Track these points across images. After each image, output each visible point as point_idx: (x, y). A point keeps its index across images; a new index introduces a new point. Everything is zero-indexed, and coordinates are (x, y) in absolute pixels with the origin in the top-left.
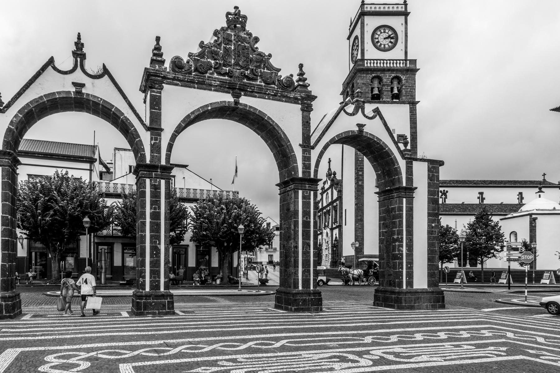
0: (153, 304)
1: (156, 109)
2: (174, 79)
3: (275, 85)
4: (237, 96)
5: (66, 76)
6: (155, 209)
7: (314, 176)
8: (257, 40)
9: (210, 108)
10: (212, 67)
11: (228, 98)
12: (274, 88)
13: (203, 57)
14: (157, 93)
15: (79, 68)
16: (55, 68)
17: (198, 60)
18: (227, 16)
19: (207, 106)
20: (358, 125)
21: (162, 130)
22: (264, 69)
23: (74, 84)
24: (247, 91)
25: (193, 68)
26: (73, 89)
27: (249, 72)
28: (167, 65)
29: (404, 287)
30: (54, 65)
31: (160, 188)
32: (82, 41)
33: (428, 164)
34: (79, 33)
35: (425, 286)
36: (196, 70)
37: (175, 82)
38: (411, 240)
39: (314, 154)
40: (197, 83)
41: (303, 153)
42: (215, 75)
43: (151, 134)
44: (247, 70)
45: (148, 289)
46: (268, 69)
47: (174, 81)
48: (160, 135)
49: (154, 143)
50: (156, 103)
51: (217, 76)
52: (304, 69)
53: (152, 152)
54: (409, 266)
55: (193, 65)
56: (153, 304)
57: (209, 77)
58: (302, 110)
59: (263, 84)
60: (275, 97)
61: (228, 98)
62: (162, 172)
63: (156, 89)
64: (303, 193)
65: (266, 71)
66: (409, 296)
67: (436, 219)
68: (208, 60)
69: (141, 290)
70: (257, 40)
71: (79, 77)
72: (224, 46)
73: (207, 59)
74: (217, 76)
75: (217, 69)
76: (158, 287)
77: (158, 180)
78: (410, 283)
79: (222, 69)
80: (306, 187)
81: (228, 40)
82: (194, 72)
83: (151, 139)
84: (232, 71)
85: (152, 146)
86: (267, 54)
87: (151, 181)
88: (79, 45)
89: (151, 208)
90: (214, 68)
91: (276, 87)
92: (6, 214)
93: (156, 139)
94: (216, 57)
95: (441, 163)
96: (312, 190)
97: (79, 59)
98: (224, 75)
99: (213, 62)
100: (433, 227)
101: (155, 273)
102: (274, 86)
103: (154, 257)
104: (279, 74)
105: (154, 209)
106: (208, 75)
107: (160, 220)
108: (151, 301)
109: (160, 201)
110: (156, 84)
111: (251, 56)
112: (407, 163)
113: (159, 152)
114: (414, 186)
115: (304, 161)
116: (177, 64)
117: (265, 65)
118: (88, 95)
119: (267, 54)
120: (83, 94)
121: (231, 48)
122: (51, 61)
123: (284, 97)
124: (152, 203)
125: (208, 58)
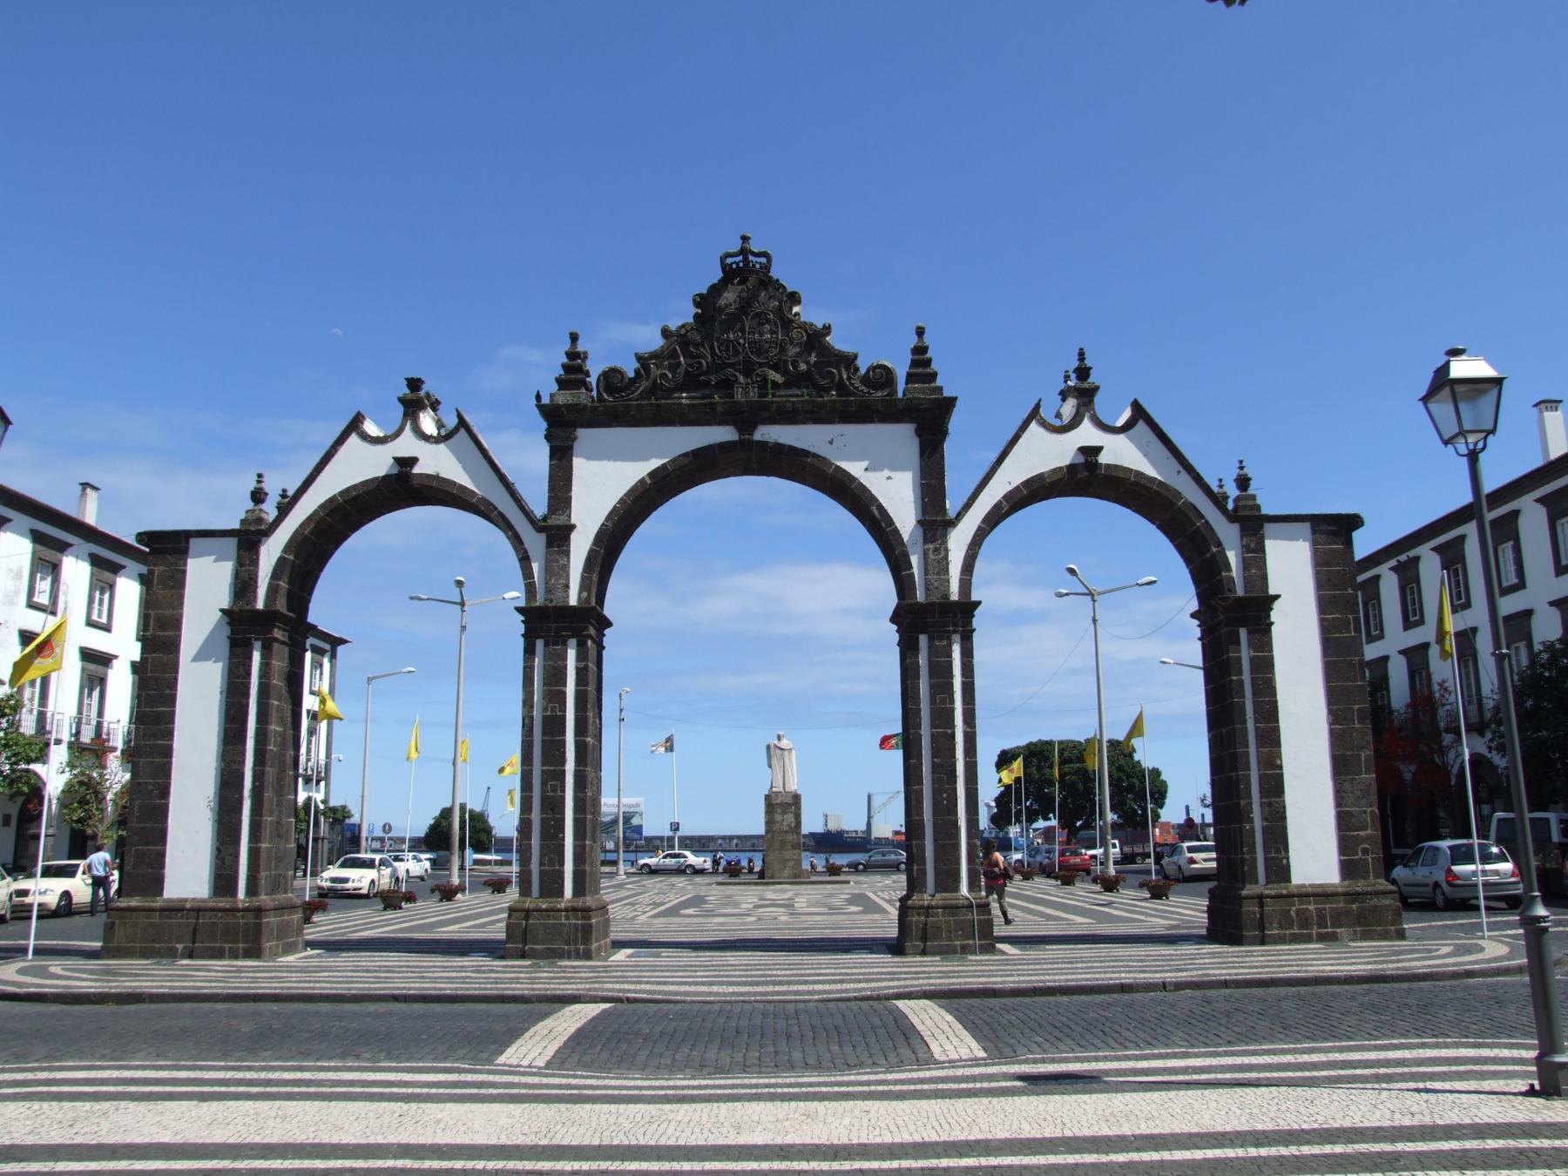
39: (958, 542)
58: (919, 433)
70: (794, 298)
78: (1280, 871)
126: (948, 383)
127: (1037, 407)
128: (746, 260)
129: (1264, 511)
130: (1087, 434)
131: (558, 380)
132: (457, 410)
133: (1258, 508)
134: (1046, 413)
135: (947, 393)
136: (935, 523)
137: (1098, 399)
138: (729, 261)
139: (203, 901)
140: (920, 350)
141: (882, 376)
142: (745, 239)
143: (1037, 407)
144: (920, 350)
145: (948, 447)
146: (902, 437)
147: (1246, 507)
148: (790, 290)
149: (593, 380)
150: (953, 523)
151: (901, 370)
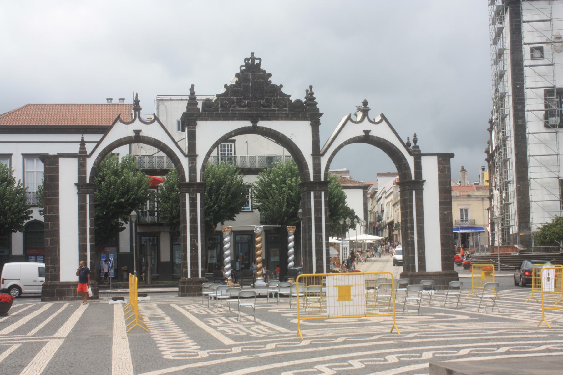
0: (194, 288)
1: (192, 141)
3: (287, 107)
4: (254, 121)
6: (193, 215)
7: (325, 178)
8: (270, 75)
10: (234, 102)
11: (247, 124)
12: (286, 110)
13: (227, 96)
14: (193, 128)
15: (137, 119)
17: (223, 98)
20: (365, 131)
21: (197, 156)
22: (277, 96)
23: (135, 131)
25: (219, 106)
27: (264, 101)
28: (200, 106)
29: (417, 270)
31: (196, 200)
32: (139, 99)
36: (222, 106)
37: (206, 118)
39: (324, 161)
42: (238, 108)
43: (189, 160)
44: (263, 100)
46: (280, 96)
48: (195, 160)
49: (191, 166)
50: (192, 137)
51: (239, 108)
52: (313, 90)
56: (194, 288)
57: (232, 110)
58: (311, 124)
59: (277, 108)
60: (287, 117)
61: (247, 124)
63: (192, 125)
67: (448, 207)
68: (231, 97)
70: (270, 75)
71: (137, 125)
73: (230, 97)
74: (239, 108)
77: (195, 194)
80: (317, 188)
81: (247, 81)
83: (189, 163)
84: (250, 103)
86: (279, 85)
87: (189, 195)
89: (190, 215)
90: (236, 103)
92: (92, 227)
96: (323, 191)
97: (137, 113)
98: (244, 106)
99: (235, 98)
100: (445, 215)
102: (286, 109)
104: (290, 98)
105: (193, 216)
106: (231, 108)
108: (192, 285)
109: (197, 210)
111: (266, 88)
114: (423, 179)
115: (315, 167)
116: (207, 103)
117: (277, 93)
118: (144, 137)
119: (279, 85)
121: (249, 85)
124: (191, 211)
125: (231, 96)
133: (420, 151)
134: (353, 117)
136: (317, 154)
142: (253, 54)
145: (321, 127)
150: (323, 155)
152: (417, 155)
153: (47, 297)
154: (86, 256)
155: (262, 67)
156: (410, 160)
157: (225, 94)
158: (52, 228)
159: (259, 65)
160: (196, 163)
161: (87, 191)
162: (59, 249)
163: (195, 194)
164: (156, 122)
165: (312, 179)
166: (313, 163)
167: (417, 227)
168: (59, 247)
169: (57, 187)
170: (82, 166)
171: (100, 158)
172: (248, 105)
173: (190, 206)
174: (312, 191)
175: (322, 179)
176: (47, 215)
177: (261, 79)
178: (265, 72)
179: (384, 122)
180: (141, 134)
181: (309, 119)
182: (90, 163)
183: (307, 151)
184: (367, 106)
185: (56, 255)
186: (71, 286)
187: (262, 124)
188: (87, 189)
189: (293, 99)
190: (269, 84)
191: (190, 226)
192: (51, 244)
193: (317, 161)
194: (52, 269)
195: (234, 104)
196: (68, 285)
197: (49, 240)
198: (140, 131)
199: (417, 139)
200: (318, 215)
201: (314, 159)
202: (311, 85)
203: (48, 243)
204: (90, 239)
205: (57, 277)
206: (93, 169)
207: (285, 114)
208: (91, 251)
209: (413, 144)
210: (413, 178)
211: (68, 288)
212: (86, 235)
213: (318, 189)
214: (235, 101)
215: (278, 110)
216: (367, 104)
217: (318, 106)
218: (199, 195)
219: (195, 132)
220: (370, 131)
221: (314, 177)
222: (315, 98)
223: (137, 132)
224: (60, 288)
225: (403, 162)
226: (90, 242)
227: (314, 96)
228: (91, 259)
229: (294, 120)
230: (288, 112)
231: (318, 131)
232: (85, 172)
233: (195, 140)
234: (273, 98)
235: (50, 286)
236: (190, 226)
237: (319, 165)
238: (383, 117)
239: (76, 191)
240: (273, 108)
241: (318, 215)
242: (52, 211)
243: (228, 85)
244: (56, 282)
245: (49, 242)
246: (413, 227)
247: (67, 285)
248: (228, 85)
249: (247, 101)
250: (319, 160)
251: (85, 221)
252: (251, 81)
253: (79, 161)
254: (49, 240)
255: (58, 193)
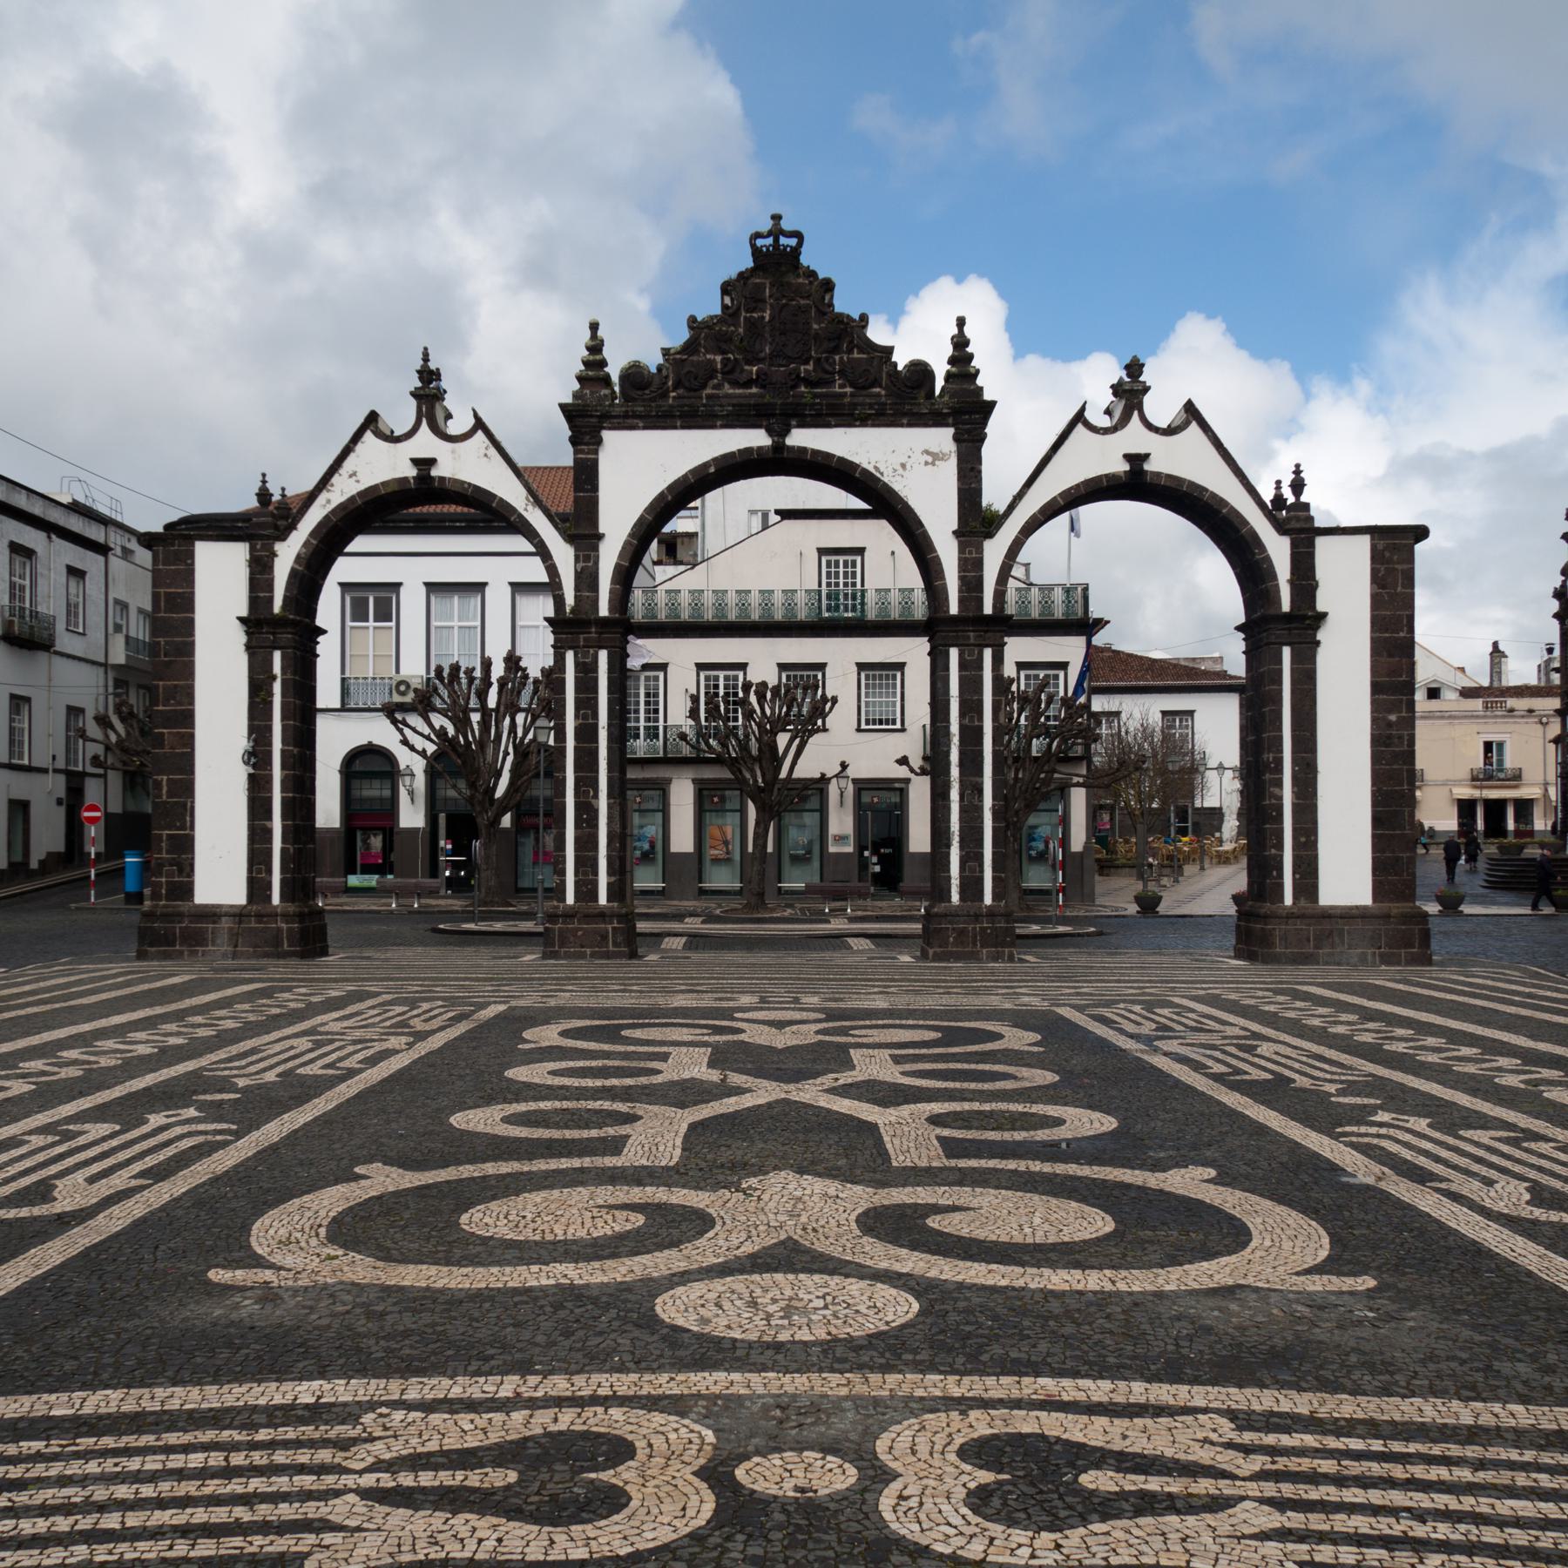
2: (626, 416)
3: (880, 386)
4: (779, 432)
5: (400, 445)
6: (585, 717)
7: (994, 606)
9: (712, 470)
11: (757, 438)
12: (878, 395)
16: (379, 434)
18: (753, 246)
19: (705, 465)
20: (1128, 457)
21: (600, 537)
22: (850, 351)
23: (416, 462)
24: (806, 416)
25: (670, 383)
26: (411, 472)
27: (810, 367)
30: (377, 427)
33: (1372, 539)
34: (426, 349)
35: (1360, 893)
37: (629, 421)
38: (1308, 765)
39: (994, 551)
40: (680, 417)
41: (961, 550)
42: (728, 389)
44: (807, 363)
45: (570, 899)
46: (861, 351)
47: (626, 421)
48: (596, 549)
50: (586, 476)
51: (731, 391)
52: (967, 331)
53: (577, 588)
54: (1303, 839)
55: (671, 376)
57: (709, 397)
58: (956, 439)
59: (848, 390)
61: (757, 438)
62: (601, 633)
63: (585, 444)
64: (961, 656)
65: (856, 355)
66: (1300, 925)
68: (708, 356)
69: (555, 903)
70: (828, 286)
72: (745, 318)
74: (731, 391)
75: (730, 371)
76: (594, 896)
79: (743, 371)
80: (969, 637)
82: (675, 388)
83: (577, 559)
84: (765, 374)
85: (579, 576)
86: (856, 316)
88: (429, 376)
89: (577, 717)
90: (723, 373)
91: (883, 392)
92: (288, 745)
93: (587, 558)
94: (724, 346)
95: (1421, 533)
96: (987, 646)
98: (748, 384)
99: (719, 358)
101: (586, 863)
102: (878, 390)
103: (582, 828)
106: (708, 391)
107: (597, 742)
109: (596, 699)
110: (586, 433)
111: (815, 326)
112: (1294, 545)
113: (594, 587)
116: (634, 376)
117: (851, 342)
118: (442, 479)
119: (856, 316)
120: (432, 479)
121: (763, 318)
122: (372, 420)
123: (905, 414)
125: (707, 352)
126: (990, 384)
127: (1083, 409)
128: (776, 240)
129: (1318, 524)
130: (1135, 438)
131: (580, 378)
132: (474, 410)
134: (1089, 415)
135: (987, 396)
137: (1148, 401)
138: (760, 242)
139: (245, 907)
140: (960, 342)
141: (921, 371)
142: (777, 218)
143: (1083, 409)
144: (960, 342)
145: (987, 450)
146: (942, 438)
147: (1298, 519)
148: (821, 276)
149: (615, 378)
151: (940, 369)
152: (1301, 531)
153: (153, 949)
154: (269, 832)
155: (805, 259)
156: (1278, 549)
157: (690, 347)
158: (172, 748)
159: (796, 251)
160: (597, 558)
161: (274, 642)
162: (193, 808)
163: (592, 651)
164: (480, 434)
165: (954, 609)
166: (960, 559)
167: (1294, 762)
168: (193, 802)
169: (190, 624)
170: (260, 569)
171: (314, 542)
172: (761, 381)
173: (578, 689)
174: (953, 646)
175: (988, 609)
176: (161, 708)
177: (802, 297)
178: (813, 274)
179: (1194, 426)
180: (434, 473)
181: (950, 420)
182: (287, 554)
183: (940, 521)
184: (1141, 379)
185: (183, 828)
186: (224, 919)
187: (802, 438)
188: (273, 634)
189: (901, 359)
190: (824, 314)
191: (576, 748)
192: (170, 794)
193: (970, 553)
194: (171, 865)
195: (712, 378)
196: (215, 915)
197: (164, 783)
198: (431, 462)
199: (1303, 480)
200: (972, 719)
201: (962, 549)
202: (961, 314)
203: (161, 790)
204: (283, 782)
205: (187, 890)
206: (293, 574)
207: (871, 406)
208: (284, 817)
209: (1291, 499)
210: (1286, 606)
211: (214, 922)
212: (271, 770)
213: (972, 641)
214: (719, 366)
215: (852, 395)
216: (1141, 373)
217: (980, 381)
218: (603, 656)
219: (595, 463)
220: (1145, 457)
221: (961, 601)
222: (971, 357)
223: (424, 464)
224: (191, 922)
225: (1254, 554)
226: (282, 792)
227: (969, 350)
228: (284, 840)
229: (902, 426)
230: (883, 399)
231: (978, 460)
232: (270, 587)
233: (595, 488)
234: (837, 358)
235: (164, 915)
236: (576, 749)
237: (979, 564)
238: (1191, 411)
239: (243, 639)
240: (837, 390)
241: (972, 719)
242: (174, 698)
243: (699, 319)
244: (183, 906)
245: (165, 789)
246: (1279, 762)
247: (212, 914)
248: (699, 319)
249: (755, 369)
250: (980, 550)
251: (269, 729)
252: (771, 305)
253: (252, 550)
254: (164, 783)
255: (192, 644)
